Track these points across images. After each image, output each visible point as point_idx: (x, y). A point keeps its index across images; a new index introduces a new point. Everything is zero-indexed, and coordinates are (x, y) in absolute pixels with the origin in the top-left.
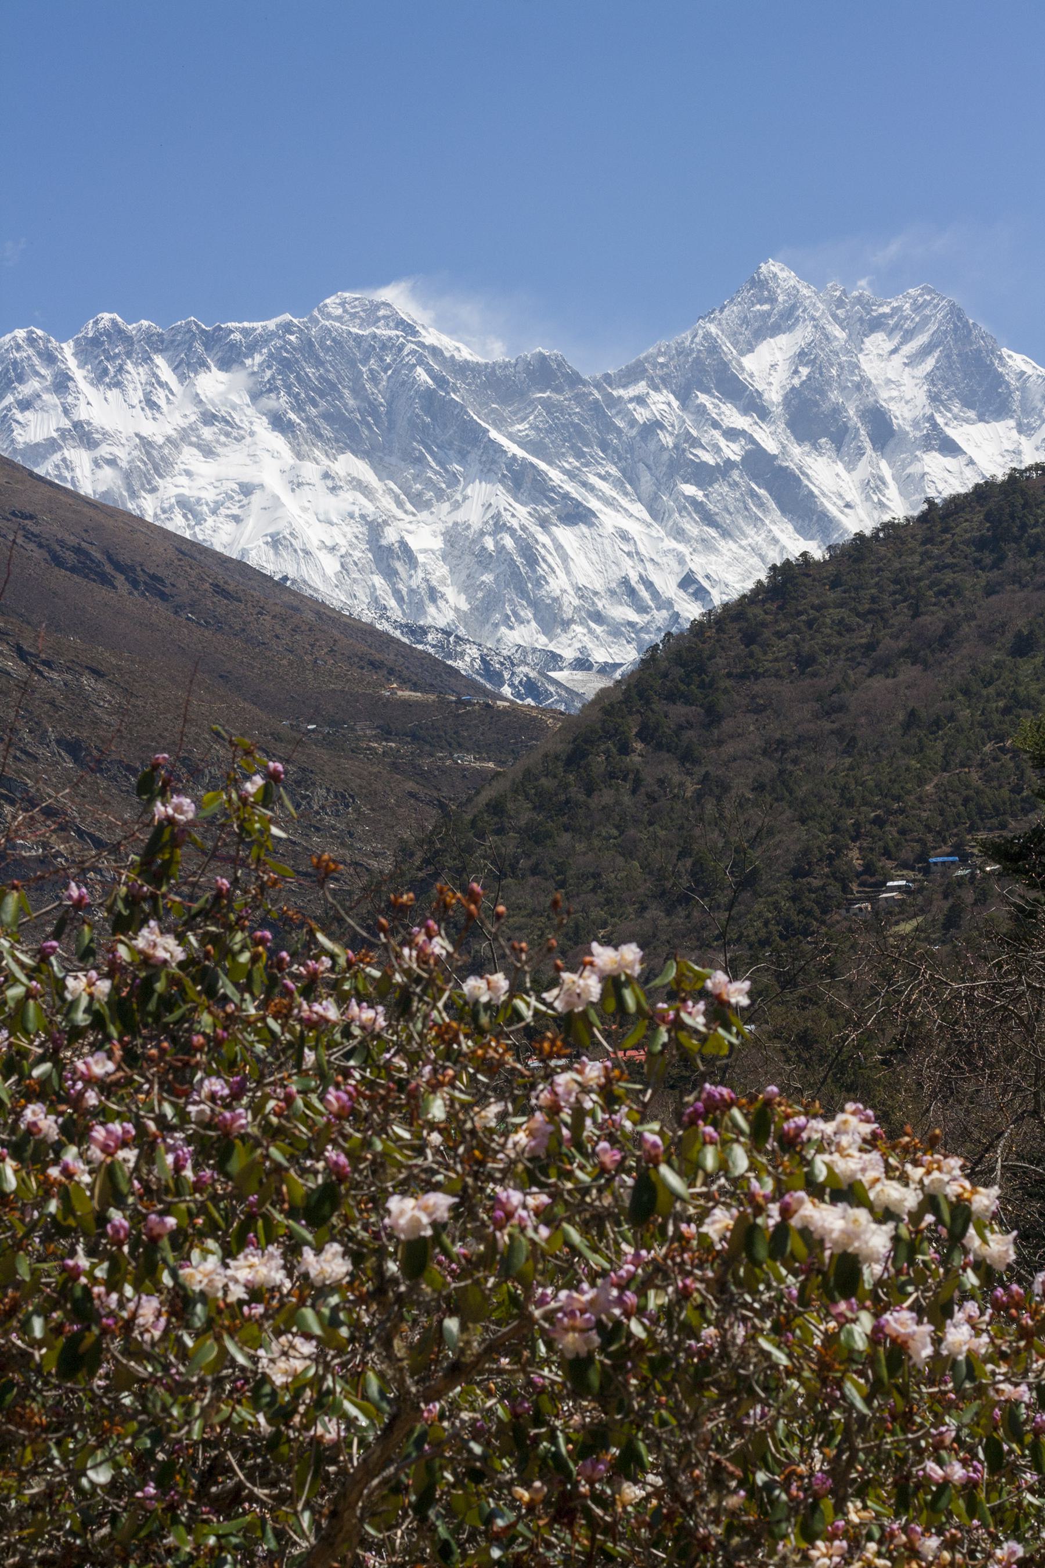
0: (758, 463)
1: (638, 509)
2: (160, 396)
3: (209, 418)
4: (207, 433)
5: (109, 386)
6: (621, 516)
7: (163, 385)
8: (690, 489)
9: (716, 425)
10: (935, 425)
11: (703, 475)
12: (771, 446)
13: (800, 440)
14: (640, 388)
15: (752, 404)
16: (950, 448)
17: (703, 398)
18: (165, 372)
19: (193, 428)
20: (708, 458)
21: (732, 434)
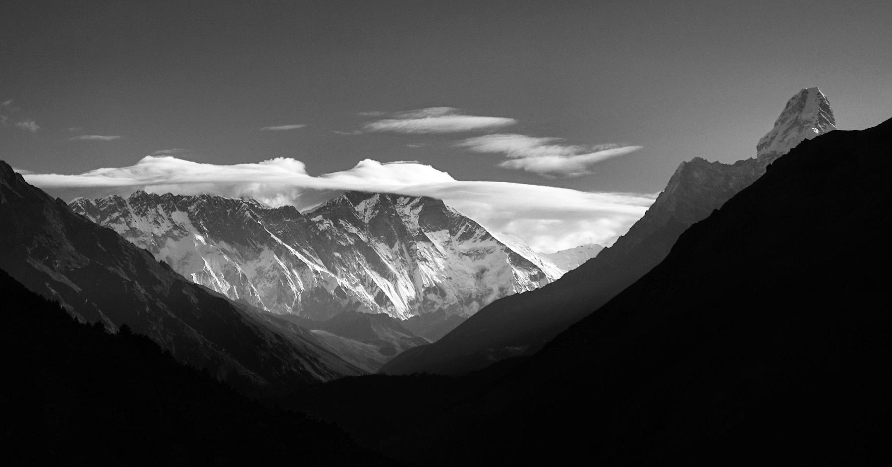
0: (359, 244)
1: (319, 261)
2: (159, 220)
3: (176, 227)
4: (176, 233)
5: (142, 216)
6: (316, 266)
7: (161, 215)
8: (337, 254)
9: (346, 231)
10: (421, 232)
11: (340, 249)
12: (364, 239)
13: (374, 236)
14: (320, 217)
15: (358, 224)
16: (426, 240)
17: (341, 222)
18: (161, 211)
19: (171, 231)
20: (343, 244)
21: (351, 235)
